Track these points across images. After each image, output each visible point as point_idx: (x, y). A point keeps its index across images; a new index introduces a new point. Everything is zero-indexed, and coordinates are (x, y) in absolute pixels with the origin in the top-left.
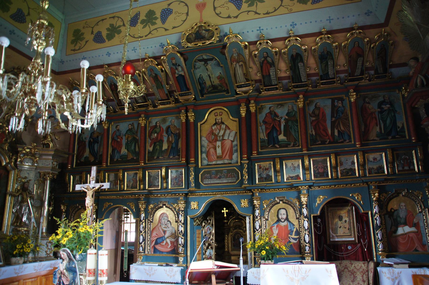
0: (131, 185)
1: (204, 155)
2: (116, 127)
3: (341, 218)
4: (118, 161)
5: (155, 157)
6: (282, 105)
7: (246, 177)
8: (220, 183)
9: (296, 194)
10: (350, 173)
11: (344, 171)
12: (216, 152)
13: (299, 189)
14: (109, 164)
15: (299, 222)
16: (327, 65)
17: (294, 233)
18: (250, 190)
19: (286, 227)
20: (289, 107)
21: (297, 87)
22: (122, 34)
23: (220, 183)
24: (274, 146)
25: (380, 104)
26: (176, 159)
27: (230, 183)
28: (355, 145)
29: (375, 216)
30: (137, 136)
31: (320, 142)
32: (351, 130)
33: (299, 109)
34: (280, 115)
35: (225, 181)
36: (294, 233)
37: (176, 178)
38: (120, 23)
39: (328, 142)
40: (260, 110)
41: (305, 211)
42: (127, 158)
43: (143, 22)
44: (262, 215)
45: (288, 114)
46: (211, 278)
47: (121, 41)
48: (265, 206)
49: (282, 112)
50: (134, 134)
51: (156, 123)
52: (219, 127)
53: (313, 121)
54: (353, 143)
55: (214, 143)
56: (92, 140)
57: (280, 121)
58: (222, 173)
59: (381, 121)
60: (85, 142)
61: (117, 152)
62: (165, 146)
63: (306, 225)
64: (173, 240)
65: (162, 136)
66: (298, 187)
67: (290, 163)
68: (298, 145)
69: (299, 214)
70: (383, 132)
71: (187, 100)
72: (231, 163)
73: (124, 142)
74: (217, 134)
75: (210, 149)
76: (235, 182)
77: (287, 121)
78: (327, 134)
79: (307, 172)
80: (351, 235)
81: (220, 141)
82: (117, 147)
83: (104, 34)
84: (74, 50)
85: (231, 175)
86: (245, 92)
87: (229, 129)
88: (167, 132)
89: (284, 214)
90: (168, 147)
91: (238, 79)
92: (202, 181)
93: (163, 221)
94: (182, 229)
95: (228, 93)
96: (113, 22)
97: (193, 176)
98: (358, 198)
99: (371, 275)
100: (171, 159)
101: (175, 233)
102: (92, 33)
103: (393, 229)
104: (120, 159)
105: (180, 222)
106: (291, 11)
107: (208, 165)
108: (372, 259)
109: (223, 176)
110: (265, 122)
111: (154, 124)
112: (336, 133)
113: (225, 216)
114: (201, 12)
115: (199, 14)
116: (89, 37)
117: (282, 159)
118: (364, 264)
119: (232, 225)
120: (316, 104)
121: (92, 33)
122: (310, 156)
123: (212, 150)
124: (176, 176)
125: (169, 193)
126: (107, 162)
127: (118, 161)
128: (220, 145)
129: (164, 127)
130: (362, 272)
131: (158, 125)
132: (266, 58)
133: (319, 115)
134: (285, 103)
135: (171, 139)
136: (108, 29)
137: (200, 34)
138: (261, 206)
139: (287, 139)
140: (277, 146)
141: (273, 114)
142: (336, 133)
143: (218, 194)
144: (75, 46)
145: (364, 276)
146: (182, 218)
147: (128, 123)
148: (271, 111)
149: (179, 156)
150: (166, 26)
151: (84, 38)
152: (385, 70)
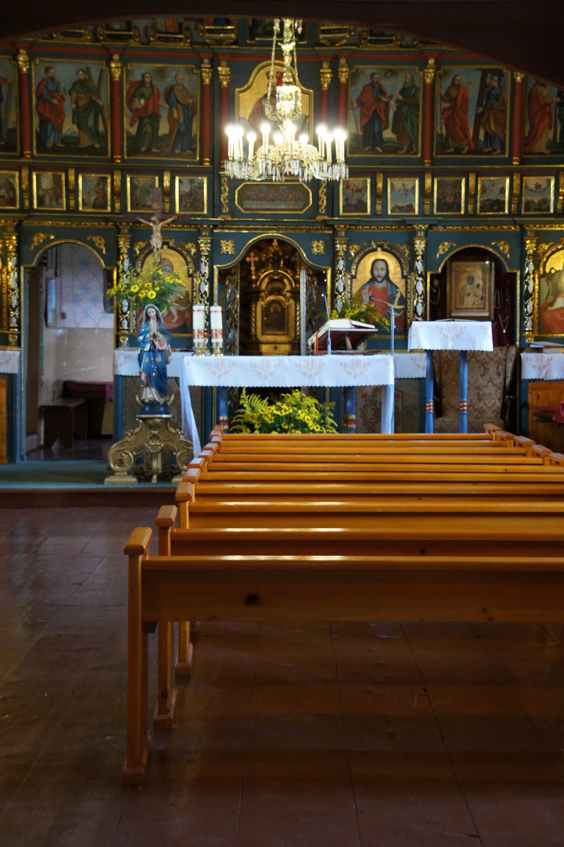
2: (47, 70)
3: (471, 280)
4: (55, 149)
5: (143, 149)
6: (394, 73)
7: (323, 202)
8: (275, 210)
10: (495, 208)
11: (487, 203)
13: (415, 228)
15: (406, 283)
17: (397, 300)
18: (331, 227)
19: (385, 290)
26: (188, 156)
28: (509, 161)
29: (526, 278)
30: (99, 98)
31: (452, 150)
32: (508, 132)
34: (388, 90)
35: (283, 207)
36: (397, 300)
39: (466, 151)
41: (419, 266)
44: (348, 268)
45: (402, 92)
46: (345, 340)
48: (353, 254)
51: (143, 76)
53: (445, 109)
54: (507, 156)
57: (387, 104)
59: (558, 121)
61: (54, 128)
62: (164, 129)
63: (420, 288)
64: (183, 308)
66: (411, 225)
67: (399, 182)
68: (415, 151)
69: (408, 270)
70: (558, 141)
71: (219, 42)
73: (68, 107)
76: (301, 210)
78: (466, 136)
80: (484, 308)
85: (295, 195)
86: (333, 42)
88: (167, 100)
89: (382, 269)
90: (171, 130)
94: (206, 288)
97: (227, 194)
98: (504, 249)
99: (510, 365)
100: (179, 155)
101: (187, 295)
103: (549, 301)
104: (60, 145)
105: (203, 276)
108: (513, 343)
109: (279, 198)
111: (138, 78)
112: (482, 137)
113: (253, 268)
117: (387, 174)
118: (501, 350)
119: (264, 286)
120: (454, 78)
124: (191, 191)
127: (55, 149)
129: (161, 86)
130: (497, 361)
131: (147, 80)
134: (400, 70)
135: (176, 115)
138: (347, 253)
139: (398, 139)
140: (379, 150)
142: (482, 137)
143: (272, 229)
145: (500, 367)
146: (205, 270)
148: (373, 81)
149: (194, 150)
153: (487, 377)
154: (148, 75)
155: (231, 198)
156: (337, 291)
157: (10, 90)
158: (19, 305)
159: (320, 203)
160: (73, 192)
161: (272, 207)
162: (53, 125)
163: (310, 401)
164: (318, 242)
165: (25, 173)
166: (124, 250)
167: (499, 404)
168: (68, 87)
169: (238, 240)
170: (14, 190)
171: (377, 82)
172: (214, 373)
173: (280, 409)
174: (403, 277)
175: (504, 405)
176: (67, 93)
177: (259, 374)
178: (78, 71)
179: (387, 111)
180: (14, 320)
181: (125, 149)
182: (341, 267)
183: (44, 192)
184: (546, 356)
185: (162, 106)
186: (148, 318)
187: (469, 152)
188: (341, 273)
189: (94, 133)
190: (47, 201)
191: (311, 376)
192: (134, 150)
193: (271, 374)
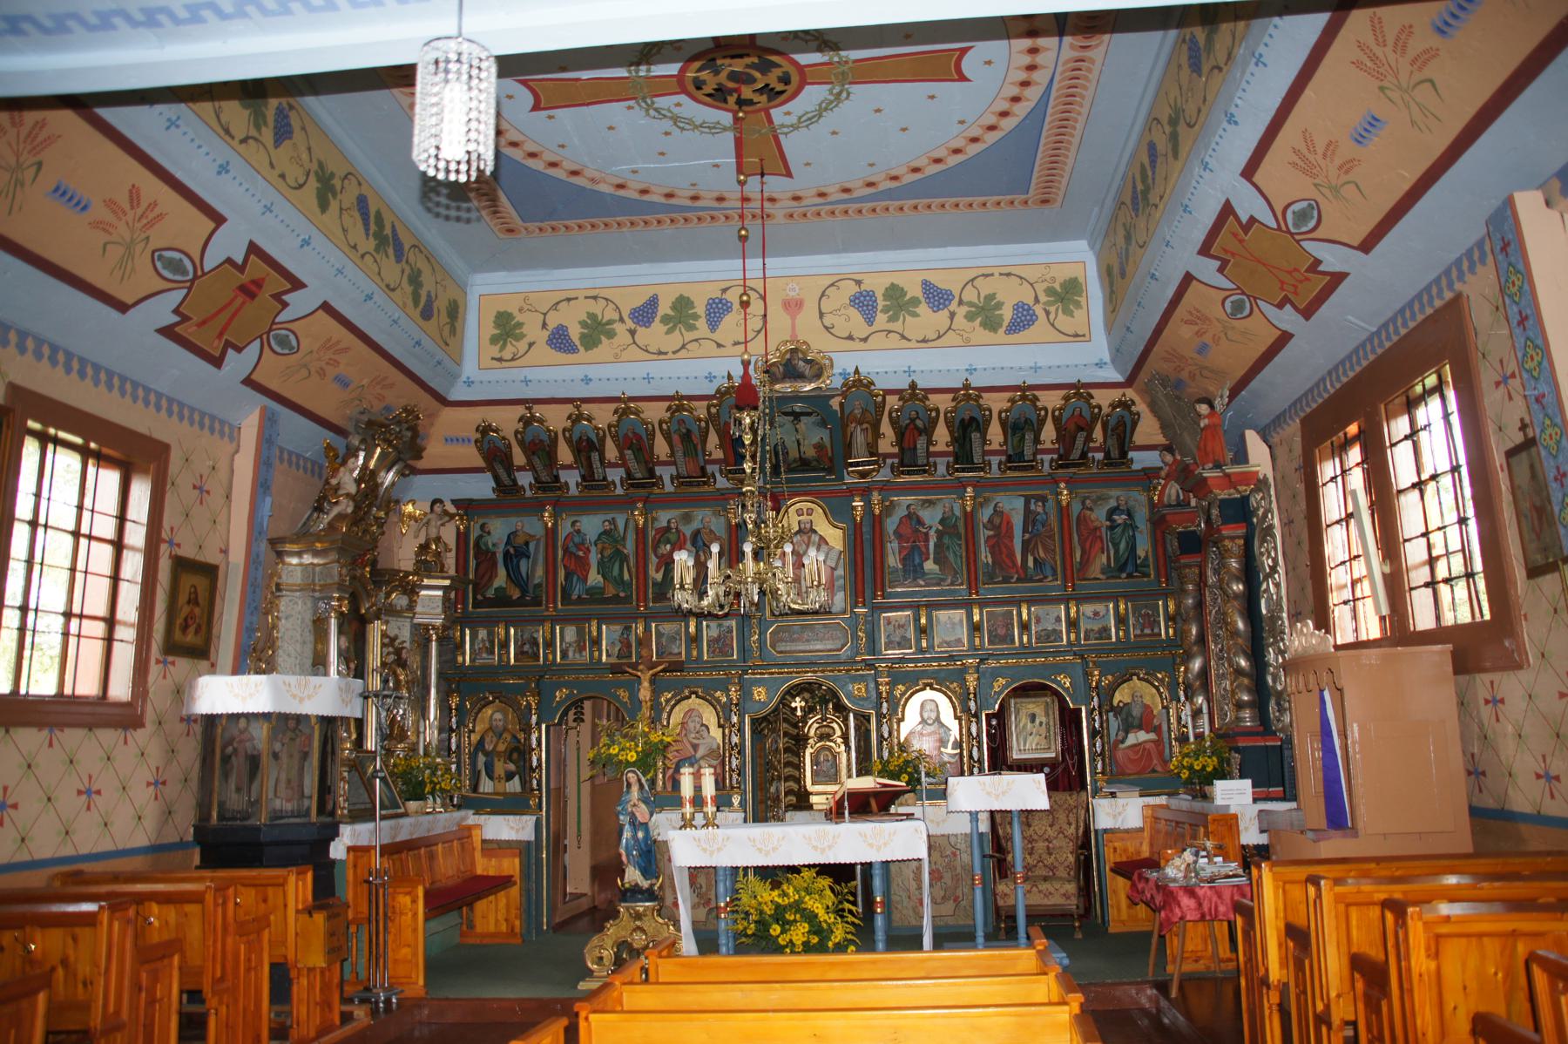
4: (580, 601)
6: (931, 503)
16: (1022, 439)
21: (963, 470)
22: (615, 340)
24: (914, 583)
25: (1112, 512)
33: (965, 512)
34: (928, 522)
37: (717, 640)
38: (610, 314)
40: (889, 509)
41: (972, 705)
43: (666, 319)
45: (942, 522)
47: (616, 356)
49: (932, 517)
57: (927, 534)
73: (594, 558)
77: (940, 535)
83: (575, 333)
84: (500, 360)
91: (854, 452)
92: (773, 646)
93: (691, 725)
96: (597, 308)
102: (544, 325)
106: (967, 343)
108: (1083, 786)
112: (1031, 563)
113: (799, 713)
114: (793, 319)
115: (789, 321)
116: (533, 330)
121: (544, 325)
122: (982, 604)
125: (704, 669)
127: (580, 601)
129: (688, 531)
132: (913, 421)
133: (1000, 526)
136: (583, 324)
137: (794, 367)
141: (912, 518)
142: (1031, 563)
144: (501, 350)
146: (735, 719)
147: (603, 517)
150: (717, 336)
151: (523, 336)
152: (1124, 454)
153: (1056, 827)
155: (762, 642)
157: (537, 546)
160: (596, 642)
163: (825, 882)
165: (548, 626)
167: (1071, 859)
169: (770, 686)
172: (705, 850)
173: (785, 894)
174: (956, 717)
175: (1077, 859)
177: (760, 850)
179: (927, 540)
184: (1120, 801)
186: (629, 786)
187: (1019, 580)
189: (620, 582)
190: (571, 654)
191: (823, 851)
193: (774, 849)
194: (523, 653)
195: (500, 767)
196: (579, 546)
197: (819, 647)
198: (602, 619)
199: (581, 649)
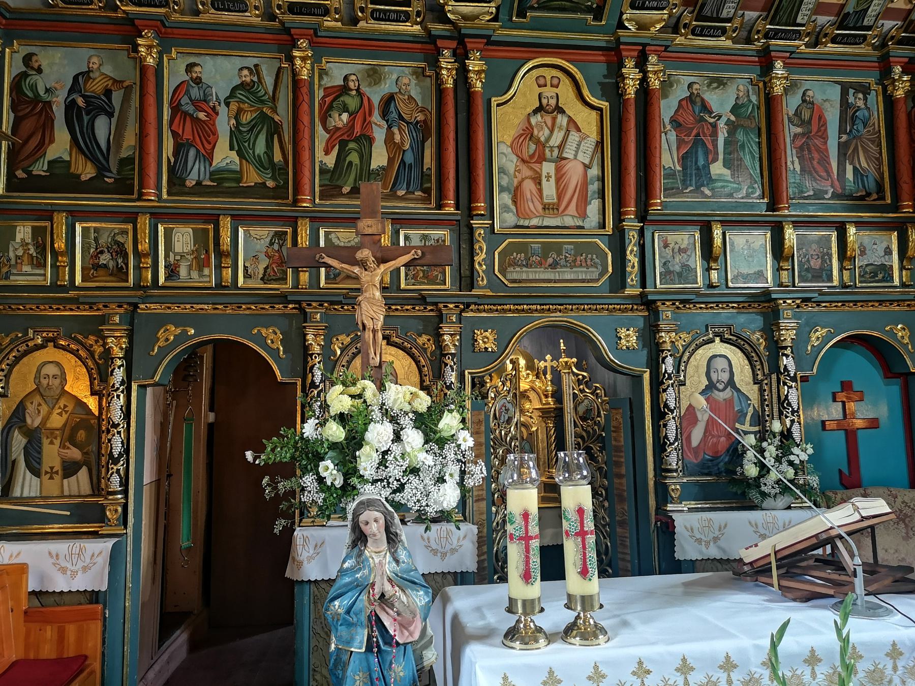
0: (261, 271)
1: (507, 198)
4: (199, 189)
6: (721, 83)
9: (759, 321)
10: (880, 276)
11: (868, 269)
12: (540, 191)
14: (165, 196)
17: (748, 418)
19: (729, 402)
20: (738, 90)
23: (549, 281)
27: (583, 281)
31: (811, 193)
36: (748, 418)
40: (667, 84)
42: (239, 180)
45: (735, 110)
50: (262, 102)
51: (346, 78)
52: (548, 119)
53: (795, 135)
55: (536, 166)
56: (80, 102)
57: (714, 126)
58: (559, 253)
60: (49, 104)
62: (379, 158)
65: (367, 124)
72: (583, 228)
73: (224, 124)
74: (542, 139)
75: (523, 180)
76: (597, 280)
77: (732, 128)
78: (828, 172)
79: (786, 265)
81: (550, 161)
82: (196, 134)
87: (579, 130)
88: (384, 114)
89: (723, 371)
90: (391, 160)
92: (503, 271)
95: (598, 17)
97: (484, 256)
100: (402, 198)
107: (517, 227)
109: (562, 262)
110: (675, 122)
112: (850, 175)
120: (804, 94)
123: (529, 186)
126: (159, 187)
128: (553, 173)
129: (376, 96)
131: (351, 85)
135: (397, 138)
140: (707, 192)
143: (556, 310)
147: (238, 62)
148: (692, 94)
149: (427, 191)
154: (353, 77)
156: (666, 405)
157: (126, 99)
158: (127, 451)
159: (629, 269)
161: (551, 276)
162: (198, 151)
164: (628, 330)
166: (317, 349)
168: (224, 94)
170: (125, 256)
171: (698, 95)
176: (223, 104)
178: (241, 69)
179: (714, 134)
180: (116, 479)
181: (317, 189)
182: (670, 369)
183: (178, 258)
185: (376, 124)
188: (670, 378)
190: (183, 272)
192: (331, 190)
194: (97, 267)
195: (52, 454)
196: (201, 103)
197: (568, 276)
198: (239, 218)
199: (202, 264)
